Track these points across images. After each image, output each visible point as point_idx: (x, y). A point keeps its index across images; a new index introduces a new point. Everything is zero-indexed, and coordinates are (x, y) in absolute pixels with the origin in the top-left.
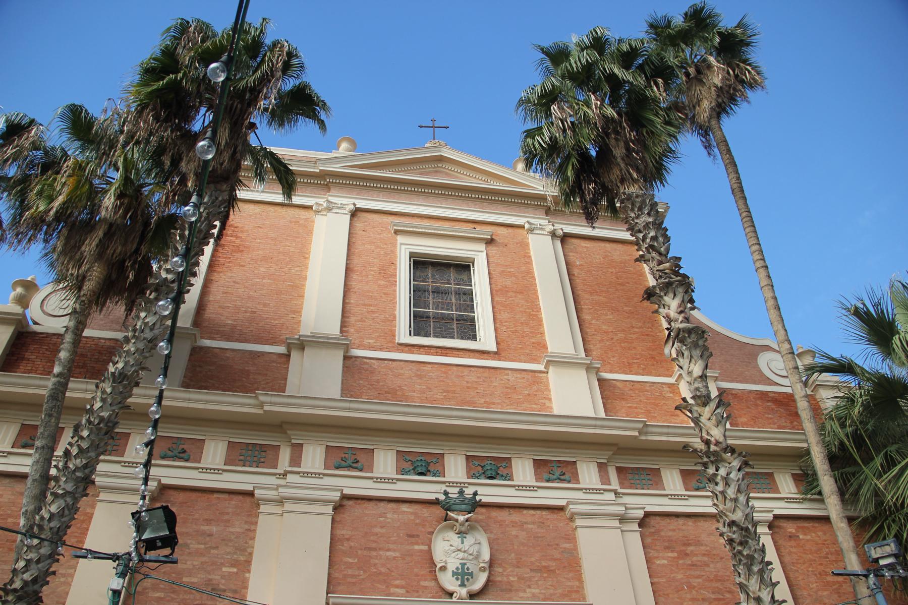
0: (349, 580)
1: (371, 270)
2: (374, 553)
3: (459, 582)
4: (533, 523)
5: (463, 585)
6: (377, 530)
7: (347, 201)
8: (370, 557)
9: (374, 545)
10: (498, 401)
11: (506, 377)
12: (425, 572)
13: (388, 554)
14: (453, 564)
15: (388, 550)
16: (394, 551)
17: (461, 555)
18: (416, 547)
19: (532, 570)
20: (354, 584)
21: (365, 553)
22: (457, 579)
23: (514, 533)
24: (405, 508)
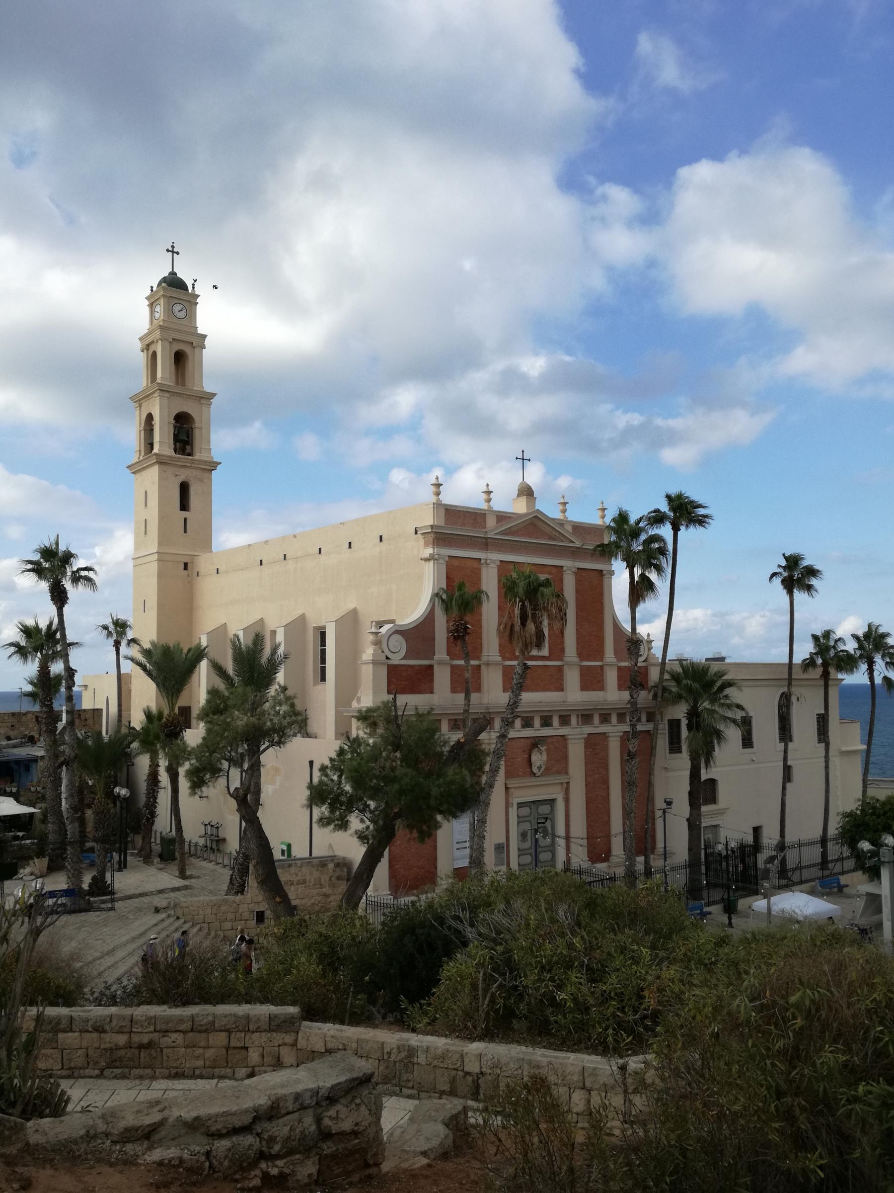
7: (496, 557)
14: (538, 765)
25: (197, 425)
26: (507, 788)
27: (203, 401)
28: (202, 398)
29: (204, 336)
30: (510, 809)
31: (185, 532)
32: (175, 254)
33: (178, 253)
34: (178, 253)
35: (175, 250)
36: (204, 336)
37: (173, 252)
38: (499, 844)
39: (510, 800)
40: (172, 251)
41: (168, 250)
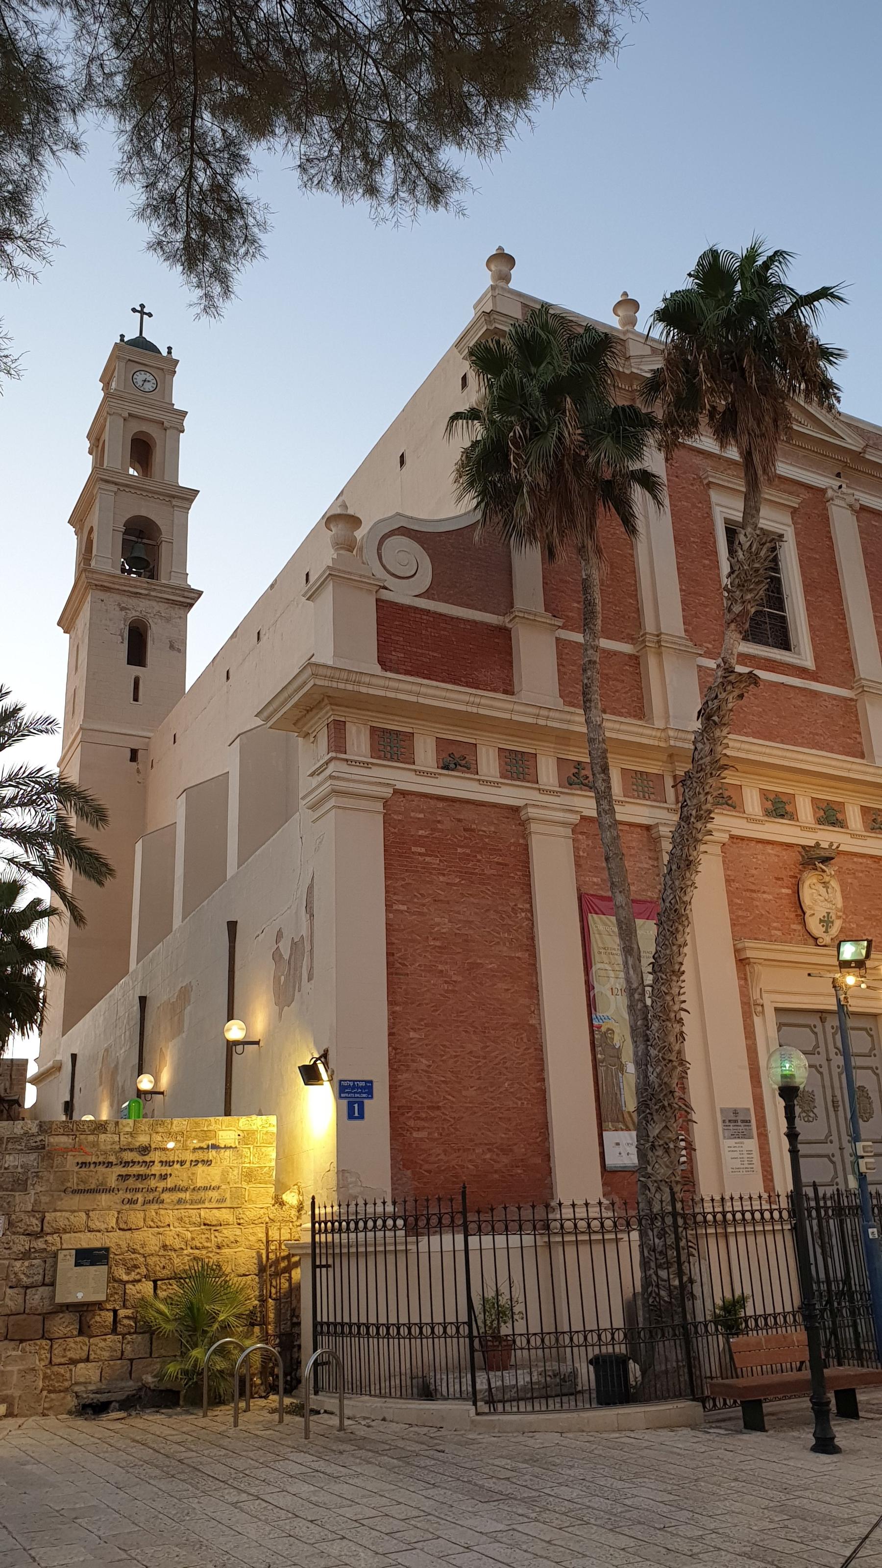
0: (741, 921)
1: (694, 542)
2: (754, 895)
3: (824, 929)
4: (862, 872)
5: (826, 932)
6: (754, 872)
8: (752, 899)
9: (753, 887)
10: (821, 732)
11: (824, 703)
12: (792, 916)
13: (765, 896)
14: (821, 913)
15: (764, 892)
16: (768, 893)
17: (829, 905)
18: (784, 891)
19: (865, 919)
20: (745, 925)
21: (748, 894)
22: (823, 926)
23: (850, 881)
24: (769, 849)
25: (164, 536)
26: (742, 963)
27: (175, 502)
28: (174, 497)
29: (184, 414)
30: (757, 1020)
31: (136, 699)
32: (145, 316)
33: (150, 315)
34: (150, 315)
35: (145, 310)
36: (184, 414)
37: (142, 313)
38: (736, 1112)
39: (755, 995)
40: (141, 311)
41: (134, 310)
